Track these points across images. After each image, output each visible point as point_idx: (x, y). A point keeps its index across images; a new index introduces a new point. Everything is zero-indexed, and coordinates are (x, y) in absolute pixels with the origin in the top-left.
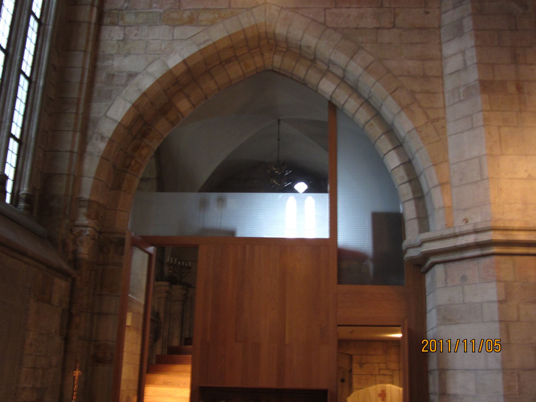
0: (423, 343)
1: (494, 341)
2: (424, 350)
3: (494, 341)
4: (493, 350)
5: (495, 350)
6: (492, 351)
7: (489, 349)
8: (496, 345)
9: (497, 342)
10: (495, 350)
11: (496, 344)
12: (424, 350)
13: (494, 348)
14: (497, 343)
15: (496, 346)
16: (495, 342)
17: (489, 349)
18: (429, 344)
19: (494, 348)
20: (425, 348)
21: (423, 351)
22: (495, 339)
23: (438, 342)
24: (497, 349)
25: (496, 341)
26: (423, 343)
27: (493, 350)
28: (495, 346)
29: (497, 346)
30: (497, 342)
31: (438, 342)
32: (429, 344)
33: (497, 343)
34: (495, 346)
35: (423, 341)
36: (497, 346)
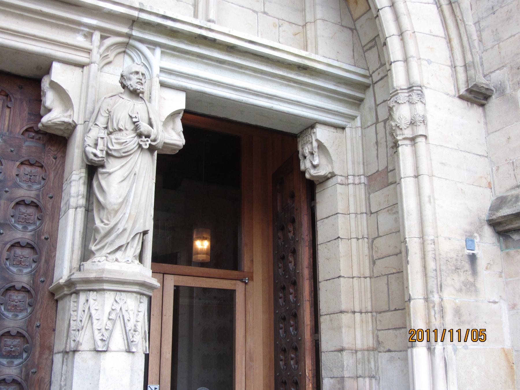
0: (410, 333)
1: (479, 331)
2: (412, 339)
3: (479, 331)
4: (479, 340)
5: (480, 339)
6: (478, 340)
7: (475, 339)
8: (481, 335)
9: (483, 332)
10: (480, 339)
11: (481, 334)
12: (412, 339)
13: (479, 337)
14: (482, 333)
15: (481, 335)
16: (481, 332)
17: (475, 339)
18: (416, 334)
19: (479, 337)
20: (412, 337)
21: (410, 340)
22: (480, 329)
23: (425, 332)
24: (483, 338)
25: (481, 330)
26: (410, 333)
27: (479, 340)
28: (480, 335)
29: (483, 336)
30: (483, 332)
31: (425, 332)
32: (416, 334)
33: (482, 333)
34: (480, 335)
35: (410, 331)
36: (483, 336)
